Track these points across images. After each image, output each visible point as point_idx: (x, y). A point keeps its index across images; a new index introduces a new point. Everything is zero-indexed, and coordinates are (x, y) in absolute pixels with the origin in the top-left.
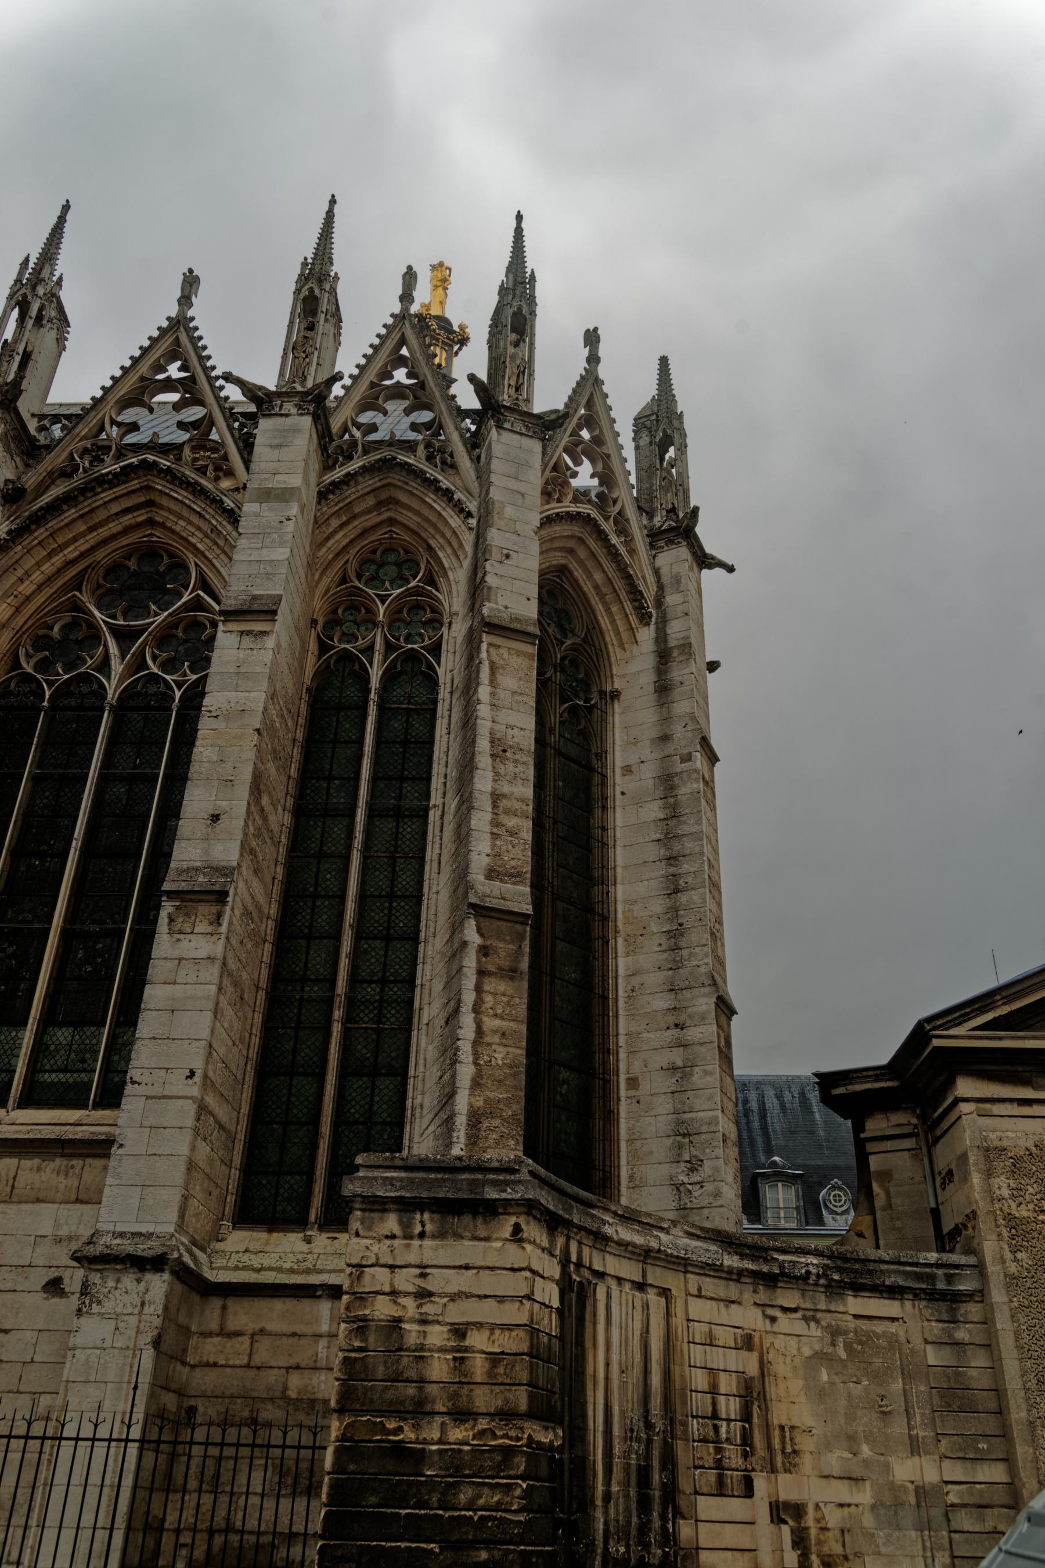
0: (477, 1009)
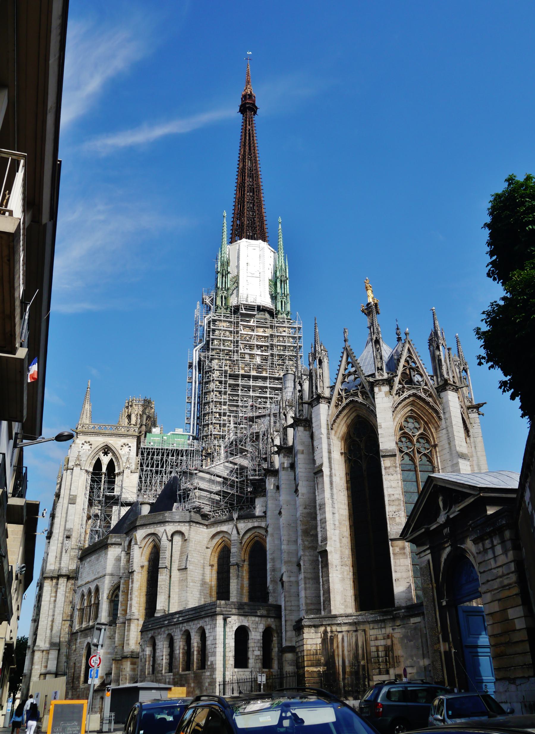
0: (322, 577)
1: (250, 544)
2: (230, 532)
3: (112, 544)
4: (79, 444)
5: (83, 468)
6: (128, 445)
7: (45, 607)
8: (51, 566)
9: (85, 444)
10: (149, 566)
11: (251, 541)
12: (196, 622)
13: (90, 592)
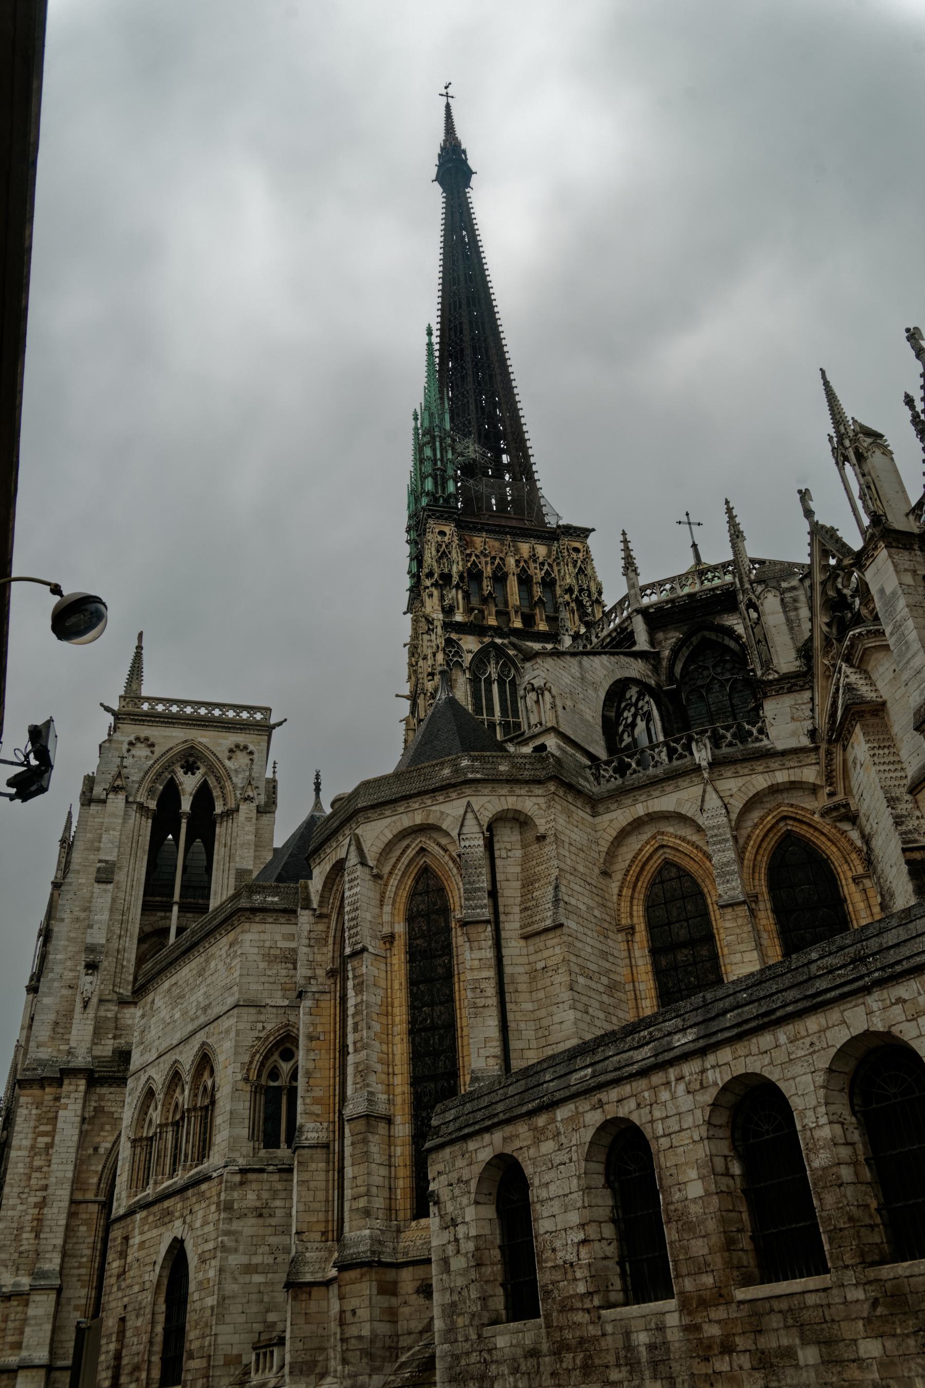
1: (764, 845)
2: (689, 810)
3: (254, 911)
4: (122, 742)
5: (131, 799)
6: (246, 748)
7: (20, 1165)
8: (41, 1049)
9: (139, 745)
10: (412, 937)
11: (766, 835)
12: (813, 1023)
13: (175, 1078)
